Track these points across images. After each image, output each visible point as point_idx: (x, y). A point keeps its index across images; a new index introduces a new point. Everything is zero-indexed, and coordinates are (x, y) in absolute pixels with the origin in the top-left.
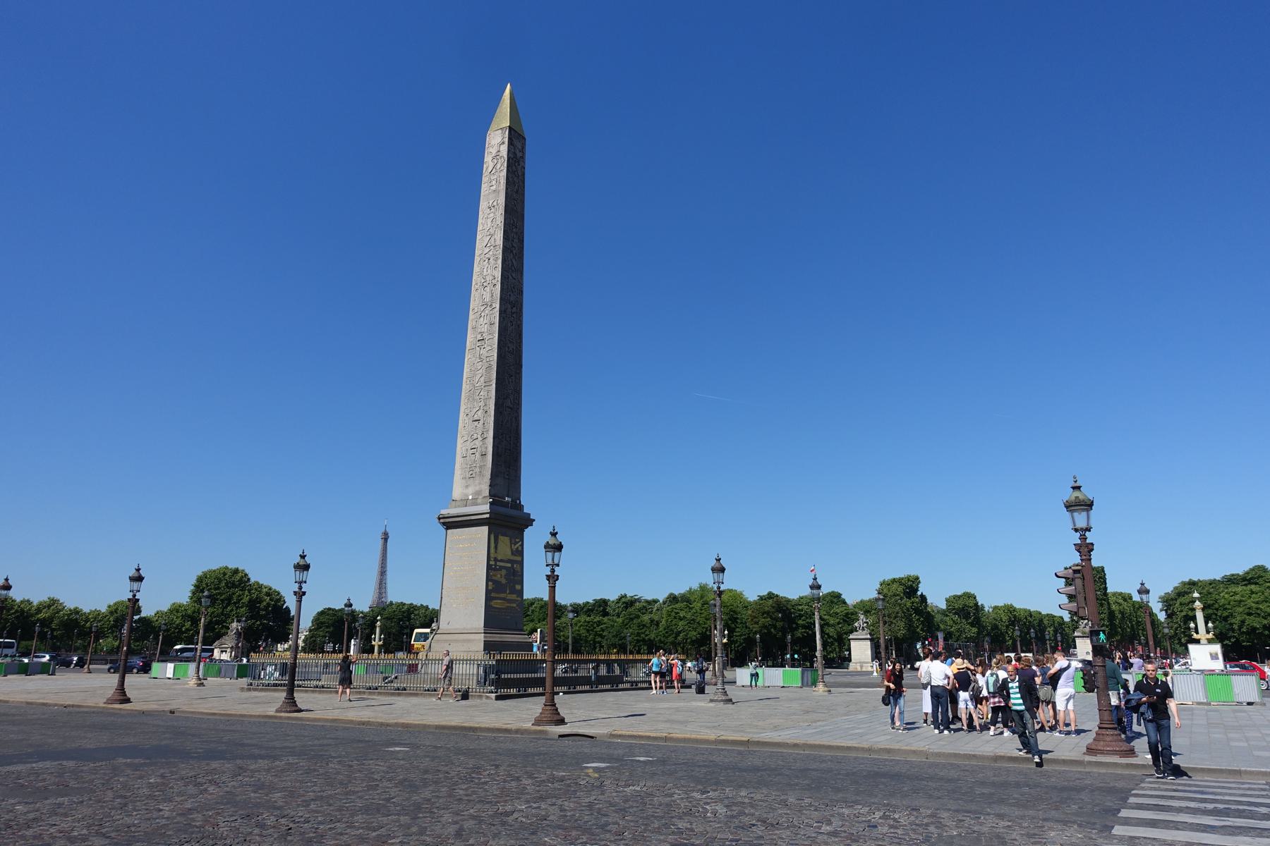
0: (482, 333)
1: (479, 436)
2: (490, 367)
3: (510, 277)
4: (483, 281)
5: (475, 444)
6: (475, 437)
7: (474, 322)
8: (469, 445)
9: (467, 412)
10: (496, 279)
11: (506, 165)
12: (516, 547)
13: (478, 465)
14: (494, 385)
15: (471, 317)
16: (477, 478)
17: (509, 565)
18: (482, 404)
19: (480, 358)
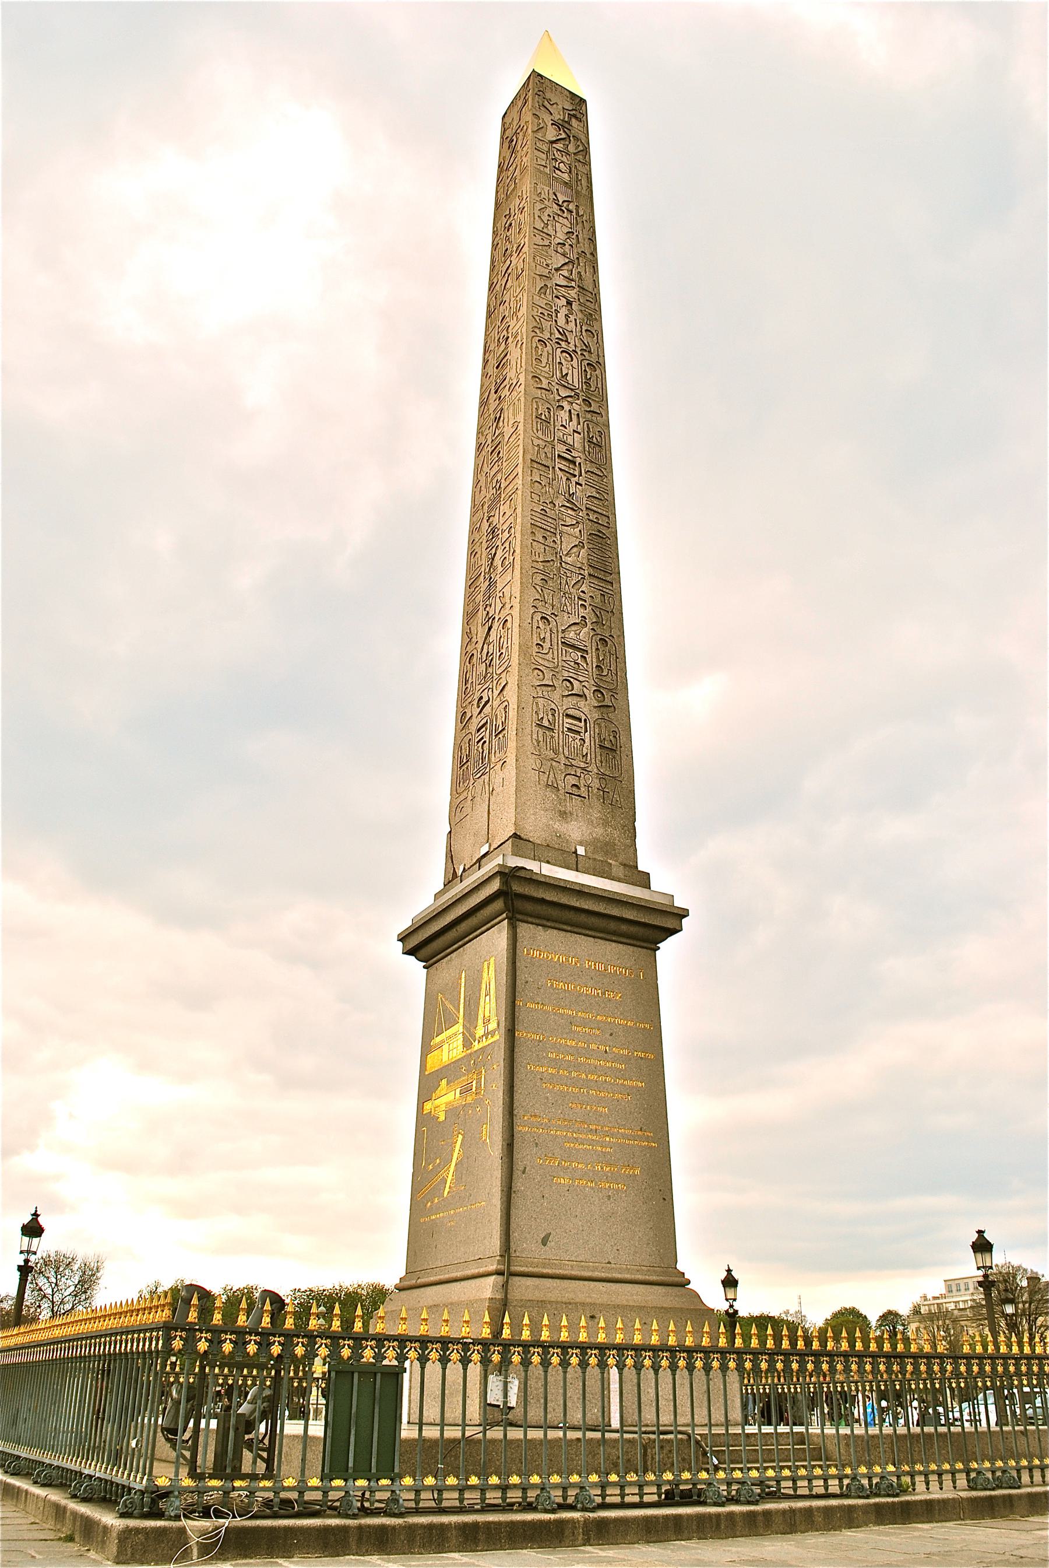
16: (597, 804)
19: (569, 501)
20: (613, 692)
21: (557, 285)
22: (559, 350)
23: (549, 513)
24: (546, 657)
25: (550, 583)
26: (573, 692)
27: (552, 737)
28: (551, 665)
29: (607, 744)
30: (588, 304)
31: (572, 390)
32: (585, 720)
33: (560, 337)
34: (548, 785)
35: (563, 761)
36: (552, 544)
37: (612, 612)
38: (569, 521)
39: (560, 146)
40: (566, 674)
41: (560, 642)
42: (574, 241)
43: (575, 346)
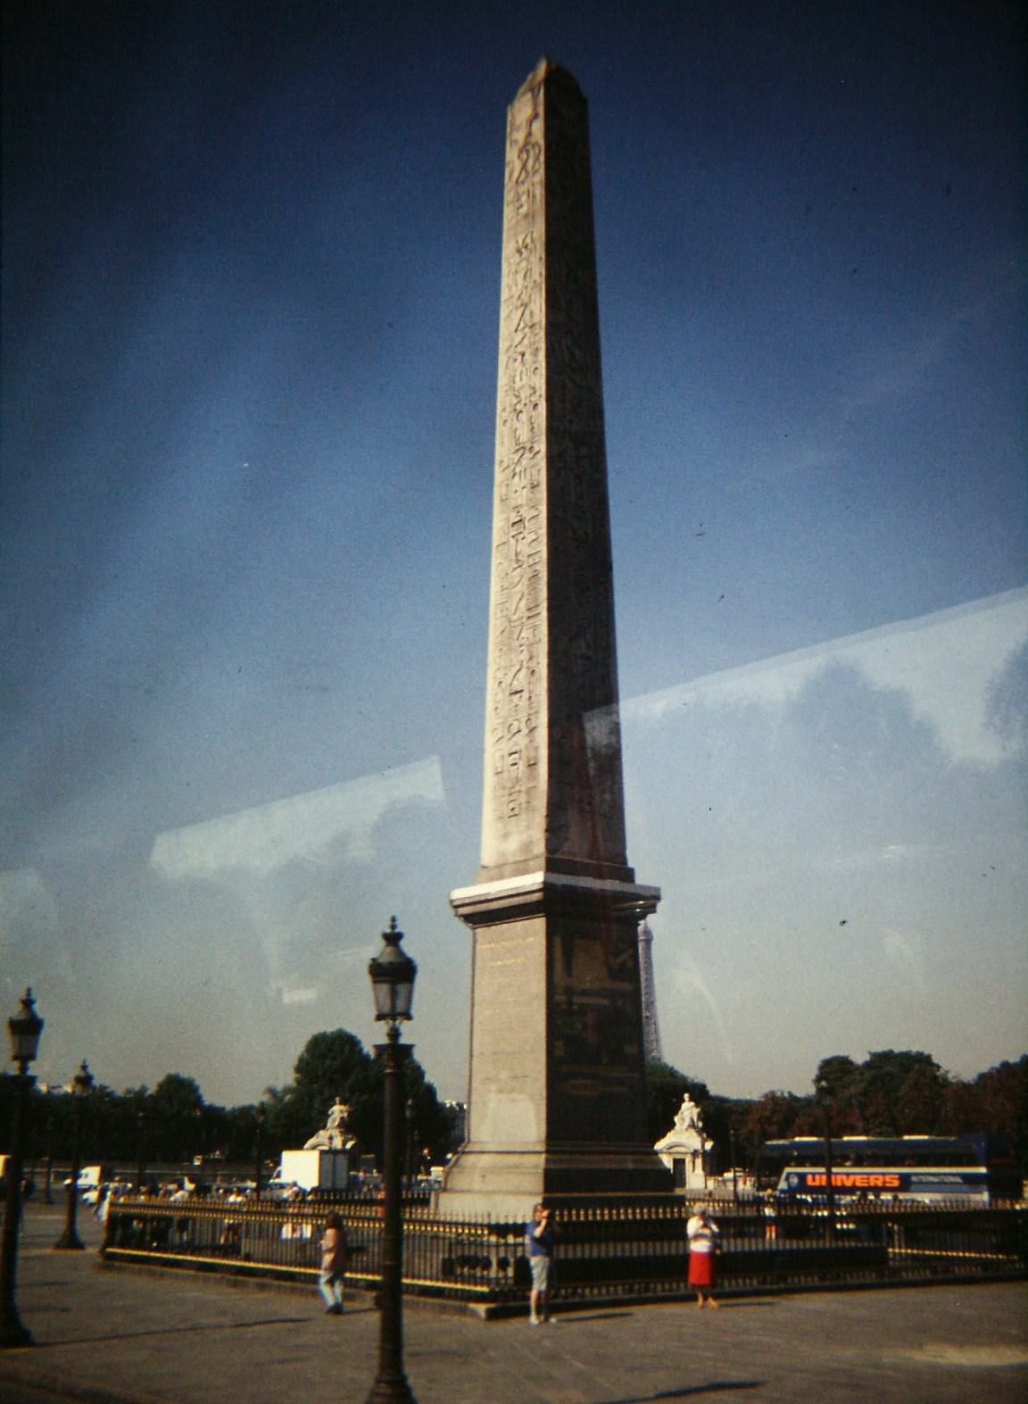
0: (517, 508)
1: (523, 726)
2: (535, 576)
3: (570, 385)
4: (515, 401)
5: (516, 744)
6: (514, 728)
7: (504, 490)
8: (506, 746)
10: (538, 394)
12: (621, 959)
13: (523, 788)
14: (544, 614)
15: (499, 476)
17: (606, 1002)
18: (525, 656)
19: (518, 561)
21: (516, 346)
28: (500, 721)
35: (507, 792)
36: (505, 613)
38: (517, 579)
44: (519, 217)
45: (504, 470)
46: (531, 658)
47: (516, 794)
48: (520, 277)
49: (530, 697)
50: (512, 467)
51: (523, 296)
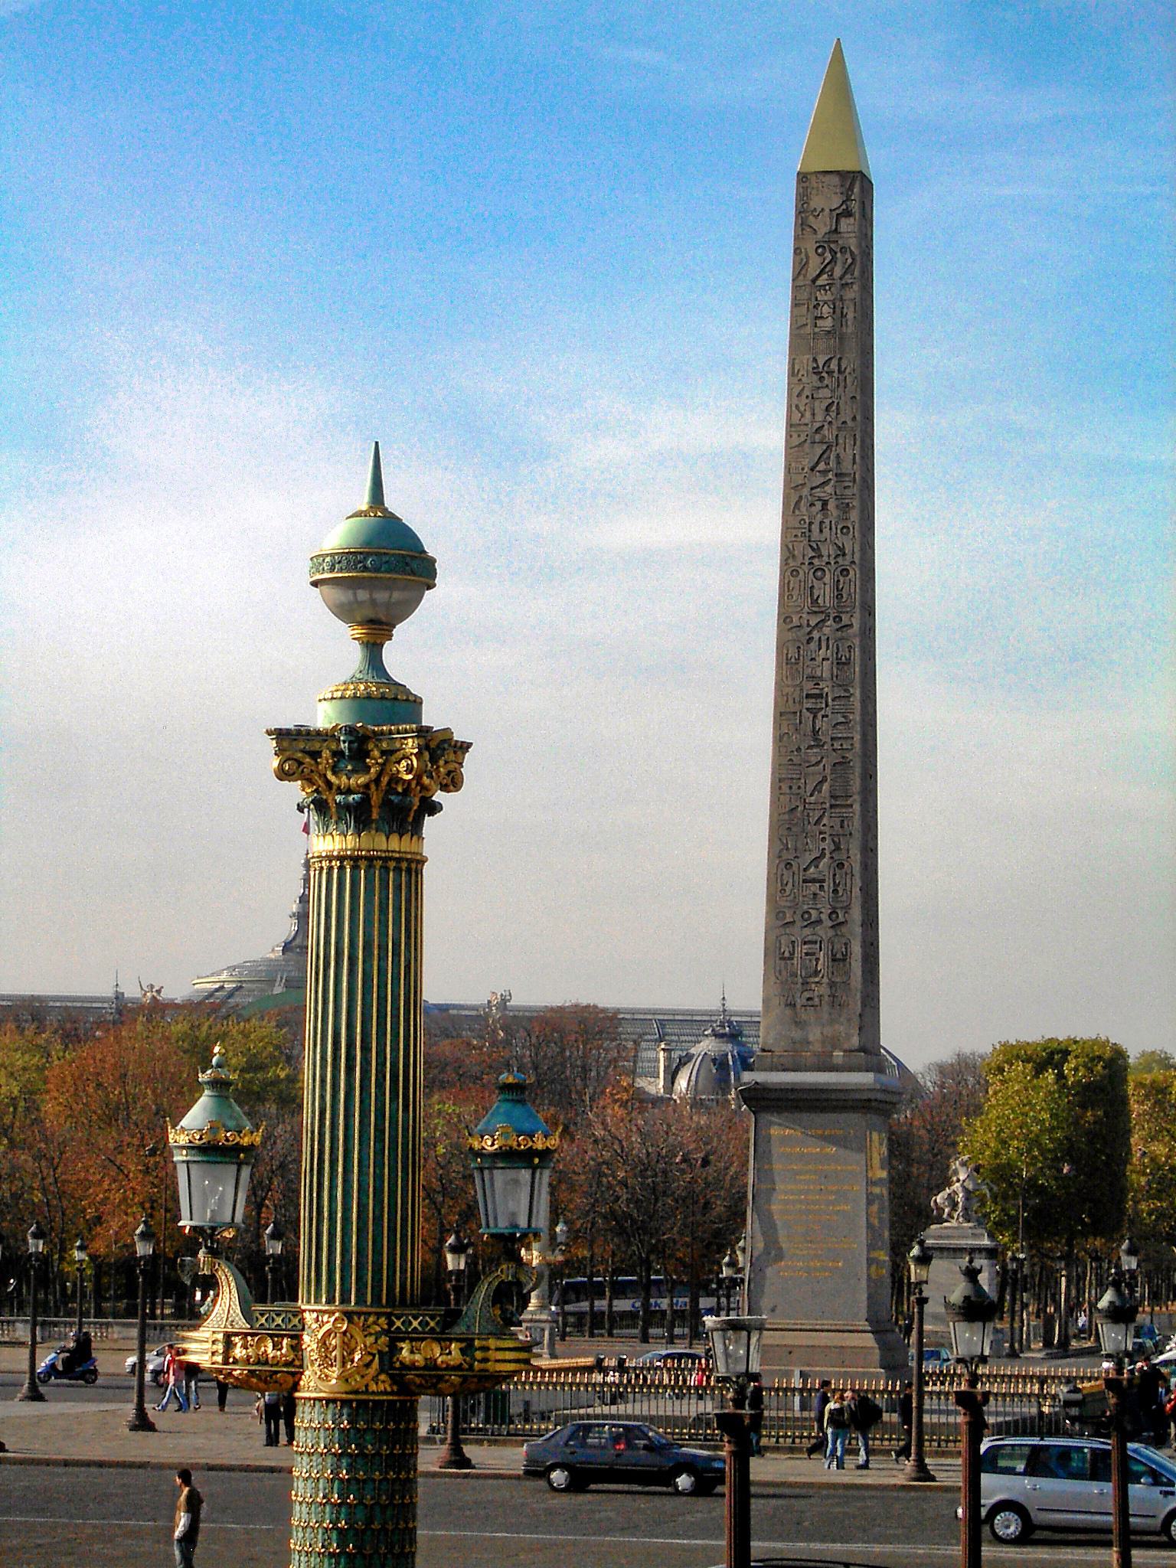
1: (824, 917)
9: (785, 855)
10: (848, 558)
11: (856, 273)
13: (825, 980)
14: (857, 807)
18: (828, 845)
19: (816, 740)
20: (847, 909)
21: (812, 489)
22: (811, 573)
23: (796, 760)
24: (788, 898)
25: (794, 829)
26: (813, 919)
27: (793, 964)
29: (839, 956)
30: (848, 492)
31: (822, 612)
32: (821, 942)
33: (814, 554)
34: (786, 1005)
35: (800, 980)
37: (851, 834)
38: (814, 760)
39: (823, 280)
40: (806, 907)
41: (801, 881)
42: (833, 415)
43: (829, 556)
44: (817, 330)
45: (792, 628)
46: (837, 848)
47: (813, 985)
48: (820, 407)
49: (835, 891)
50: (809, 629)
51: (825, 431)
